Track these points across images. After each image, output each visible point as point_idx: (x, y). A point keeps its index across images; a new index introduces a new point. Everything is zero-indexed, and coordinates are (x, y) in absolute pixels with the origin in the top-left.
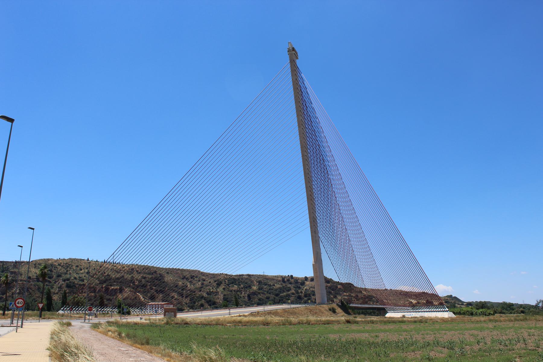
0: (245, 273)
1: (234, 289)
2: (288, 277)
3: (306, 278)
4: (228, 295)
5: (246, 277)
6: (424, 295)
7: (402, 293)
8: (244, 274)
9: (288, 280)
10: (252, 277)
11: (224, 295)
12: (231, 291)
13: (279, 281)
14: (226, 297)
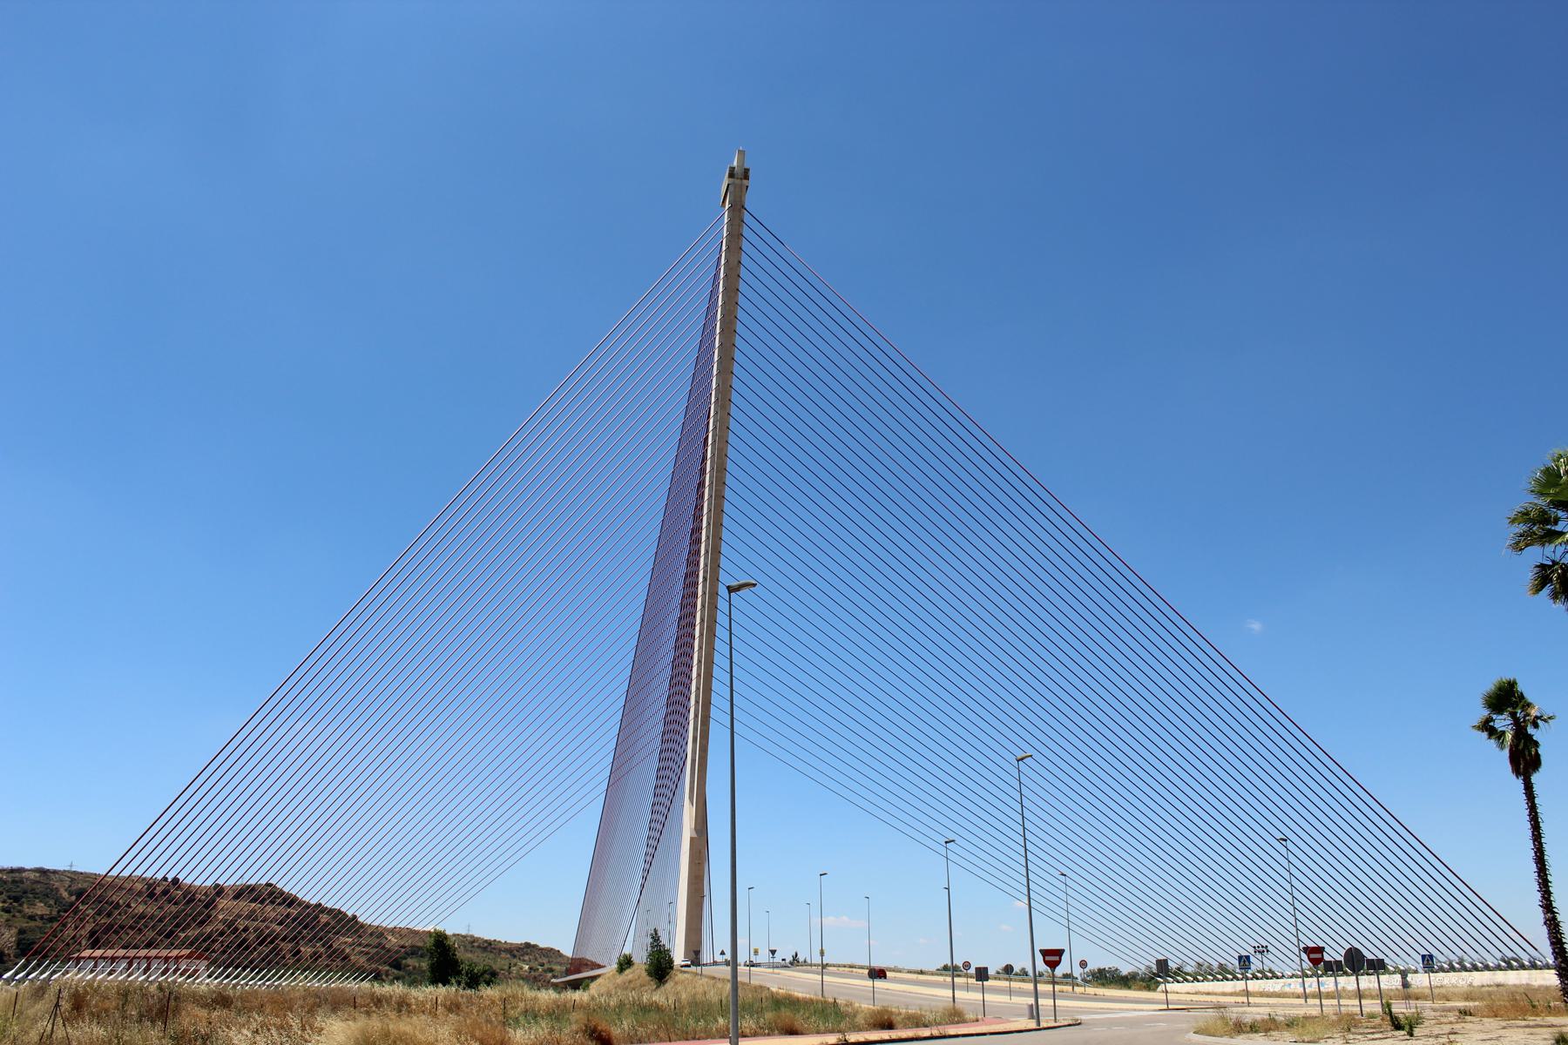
0: (29, 864)
1: (39, 913)
2: (164, 883)
3: (219, 890)
4: (32, 930)
5: (32, 876)
6: (529, 951)
7: (476, 944)
8: (26, 867)
9: (165, 892)
10: (52, 876)
11: (21, 932)
12: (32, 918)
13: (140, 893)
14: (30, 936)
